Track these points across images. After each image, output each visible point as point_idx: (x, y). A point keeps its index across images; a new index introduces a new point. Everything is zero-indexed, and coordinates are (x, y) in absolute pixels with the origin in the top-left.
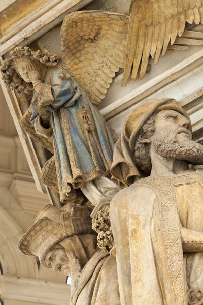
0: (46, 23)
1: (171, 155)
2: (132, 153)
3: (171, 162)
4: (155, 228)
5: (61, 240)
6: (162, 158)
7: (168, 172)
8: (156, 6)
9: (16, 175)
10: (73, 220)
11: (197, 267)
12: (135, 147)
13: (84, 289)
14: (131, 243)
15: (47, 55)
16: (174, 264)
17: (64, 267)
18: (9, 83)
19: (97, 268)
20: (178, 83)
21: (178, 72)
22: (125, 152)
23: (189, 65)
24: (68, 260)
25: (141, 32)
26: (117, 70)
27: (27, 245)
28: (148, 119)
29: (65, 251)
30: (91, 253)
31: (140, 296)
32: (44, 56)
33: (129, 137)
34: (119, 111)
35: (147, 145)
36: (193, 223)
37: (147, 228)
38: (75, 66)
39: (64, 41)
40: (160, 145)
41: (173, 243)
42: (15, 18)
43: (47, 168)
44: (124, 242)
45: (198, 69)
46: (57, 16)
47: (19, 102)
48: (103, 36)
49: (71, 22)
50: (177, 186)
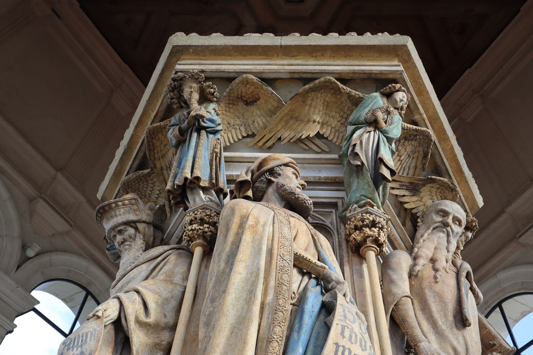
0: (226, 71)
5: (139, 221)
6: (278, 196)
8: (307, 108)
9: (43, 195)
10: (154, 214)
13: (145, 264)
15: (215, 89)
17: (127, 243)
18: (170, 91)
19: (167, 253)
24: (134, 240)
25: (285, 118)
26: (250, 133)
27: (107, 211)
28: (281, 166)
29: (136, 231)
30: (156, 244)
31: (240, 273)
32: (211, 88)
33: (258, 170)
35: (270, 182)
38: (224, 112)
39: (230, 90)
42: (197, 57)
43: (135, 176)
46: (237, 71)
47: (157, 114)
48: (257, 105)
49: (245, 80)
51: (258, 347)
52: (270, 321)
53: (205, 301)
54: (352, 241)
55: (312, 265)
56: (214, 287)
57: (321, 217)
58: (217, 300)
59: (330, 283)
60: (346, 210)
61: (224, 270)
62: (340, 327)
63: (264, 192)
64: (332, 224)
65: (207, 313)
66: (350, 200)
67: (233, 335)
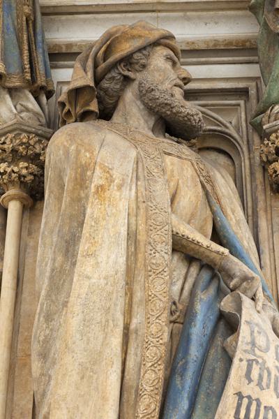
1: (164, 110)
2: (98, 80)
3: (153, 118)
4: (137, 197)
6: (142, 107)
7: (146, 129)
11: (174, 271)
12: (106, 74)
14: (92, 203)
16: (157, 254)
20: (158, 17)
21: (168, 3)
22: (90, 74)
23: (187, 3)
28: (144, 48)
31: (88, 278)
34: (63, 11)
35: (127, 80)
36: (179, 211)
37: (125, 192)
40: (153, 90)
41: (161, 227)
44: (76, 195)
45: (194, 13)
50: (165, 153)
51: (124, 400)
52: (139, 359)
53: (36, 320)
54: (271, 176)
55: (202, 250)
56: (48, 296)
57: (220, 119)
58: (56, 317)
59: (232, 279)
60: (263, 112)
61: (62, 266)
62: (245, 363)
63: (118, 98)
64: (238, 131)
65: (42, 338)
66: (269, 95)
67: (85, 380)
